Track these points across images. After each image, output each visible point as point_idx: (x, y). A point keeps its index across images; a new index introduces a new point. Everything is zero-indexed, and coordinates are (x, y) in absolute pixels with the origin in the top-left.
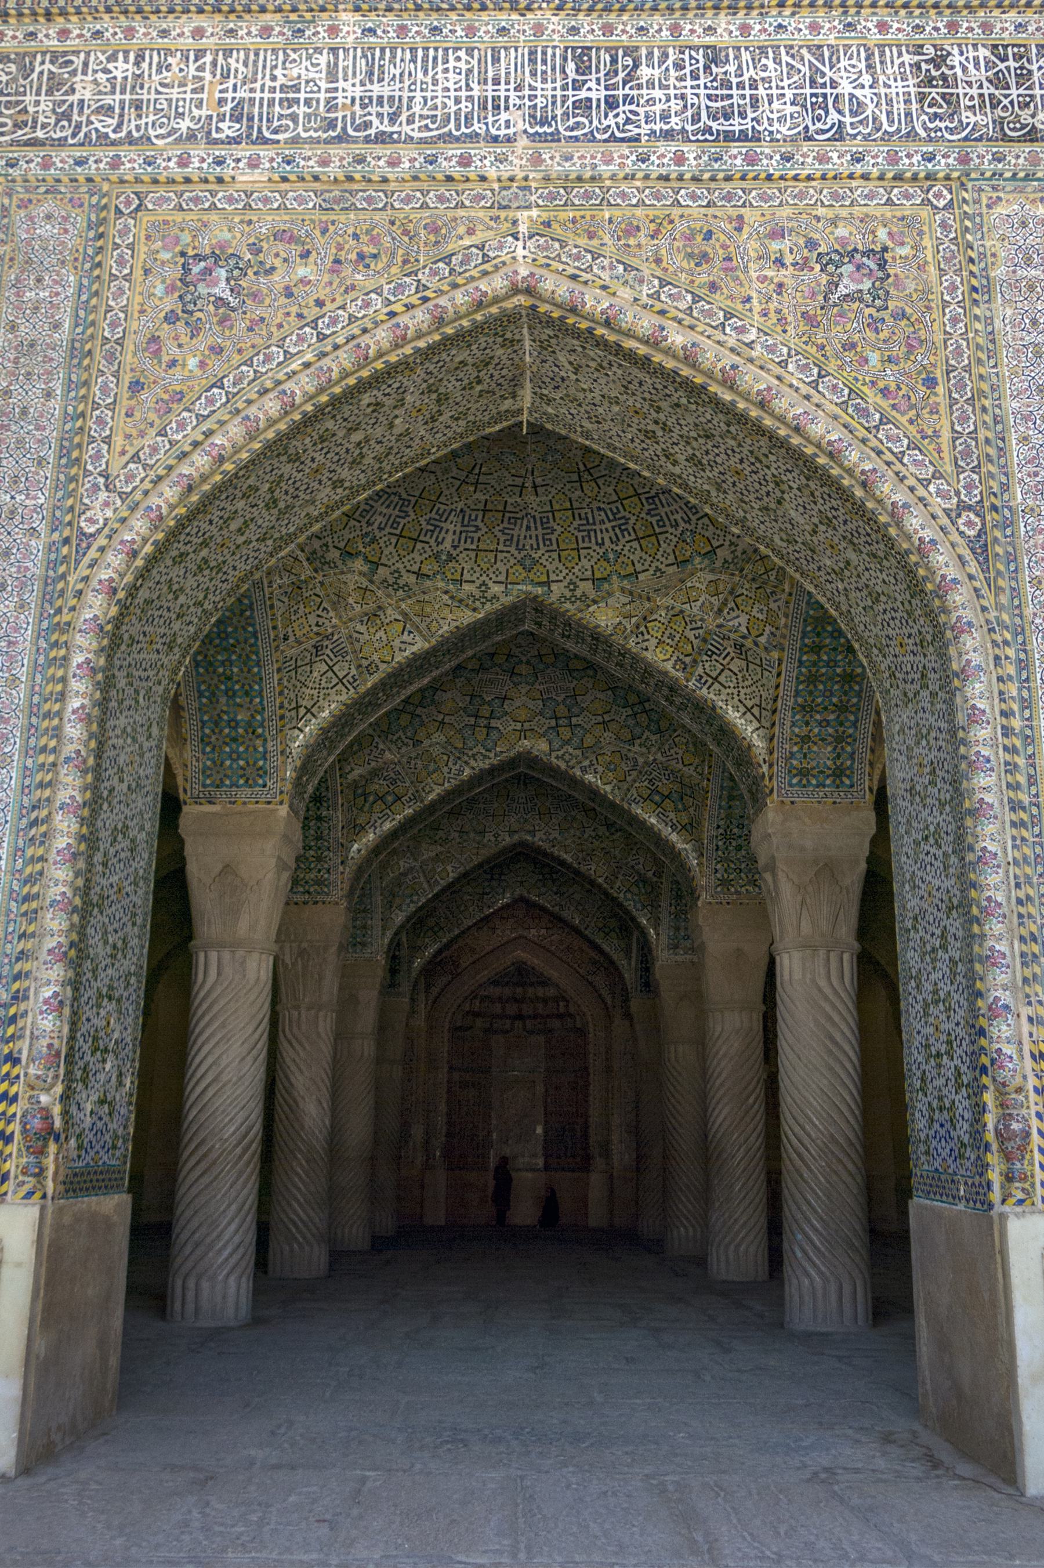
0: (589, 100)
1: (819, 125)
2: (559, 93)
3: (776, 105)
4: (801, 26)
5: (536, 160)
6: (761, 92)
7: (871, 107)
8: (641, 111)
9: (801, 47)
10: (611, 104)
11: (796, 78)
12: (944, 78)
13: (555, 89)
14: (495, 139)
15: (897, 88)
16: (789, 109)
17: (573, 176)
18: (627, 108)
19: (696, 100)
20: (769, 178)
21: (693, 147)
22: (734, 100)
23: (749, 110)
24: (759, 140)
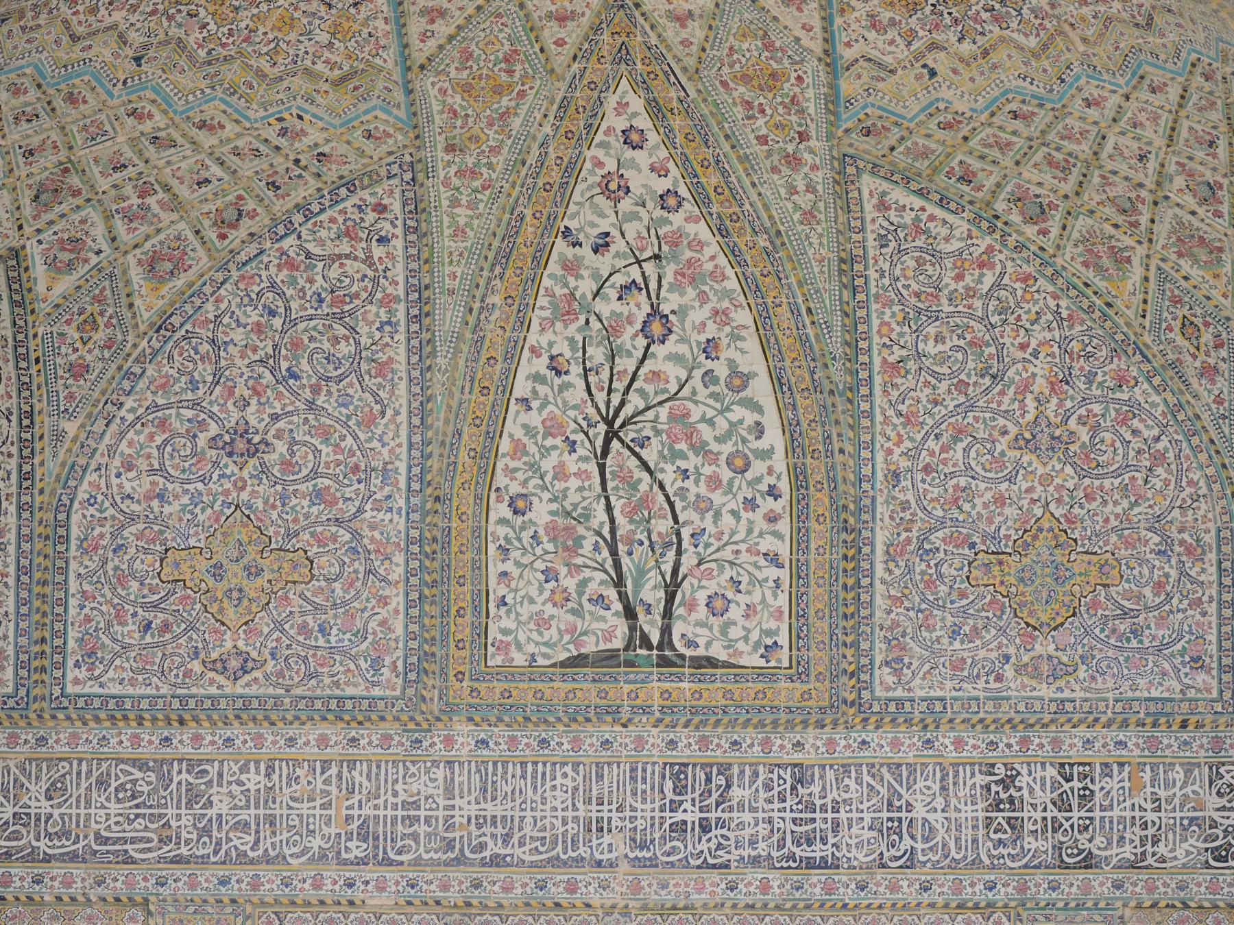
0: (685, 822)
1: (893, 852)
2: (657, 814)
3: (854, 830)
4: (883, 742)
5: (636, 888)
6: (843, 815)
7: (942, 831)
8: (731, 835)
9: (882, 765)
10: (705, 828)
11: (874, 801)
12: (1011, 800)
13: (653, 810)
14: (599, 864)
15: (967, 812)
16: (868, 834)
17: (668, 905)
18: (719, 832)
19: (782, 825)
20: (845, 906)
21: (777, 874)
22: (819, 824)
23: (830, 835)
24: (837, 867)
